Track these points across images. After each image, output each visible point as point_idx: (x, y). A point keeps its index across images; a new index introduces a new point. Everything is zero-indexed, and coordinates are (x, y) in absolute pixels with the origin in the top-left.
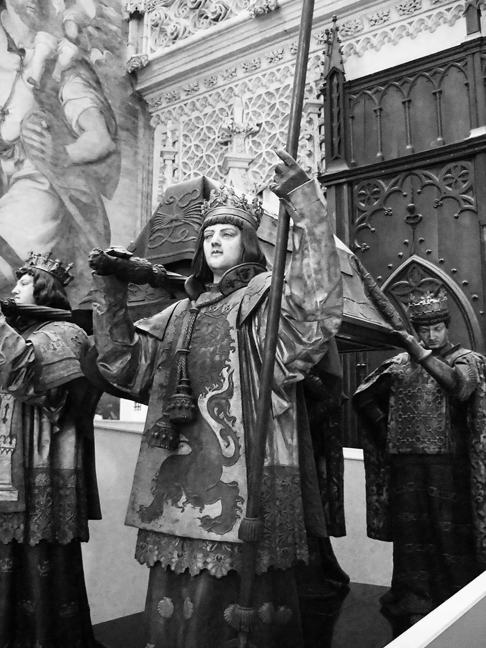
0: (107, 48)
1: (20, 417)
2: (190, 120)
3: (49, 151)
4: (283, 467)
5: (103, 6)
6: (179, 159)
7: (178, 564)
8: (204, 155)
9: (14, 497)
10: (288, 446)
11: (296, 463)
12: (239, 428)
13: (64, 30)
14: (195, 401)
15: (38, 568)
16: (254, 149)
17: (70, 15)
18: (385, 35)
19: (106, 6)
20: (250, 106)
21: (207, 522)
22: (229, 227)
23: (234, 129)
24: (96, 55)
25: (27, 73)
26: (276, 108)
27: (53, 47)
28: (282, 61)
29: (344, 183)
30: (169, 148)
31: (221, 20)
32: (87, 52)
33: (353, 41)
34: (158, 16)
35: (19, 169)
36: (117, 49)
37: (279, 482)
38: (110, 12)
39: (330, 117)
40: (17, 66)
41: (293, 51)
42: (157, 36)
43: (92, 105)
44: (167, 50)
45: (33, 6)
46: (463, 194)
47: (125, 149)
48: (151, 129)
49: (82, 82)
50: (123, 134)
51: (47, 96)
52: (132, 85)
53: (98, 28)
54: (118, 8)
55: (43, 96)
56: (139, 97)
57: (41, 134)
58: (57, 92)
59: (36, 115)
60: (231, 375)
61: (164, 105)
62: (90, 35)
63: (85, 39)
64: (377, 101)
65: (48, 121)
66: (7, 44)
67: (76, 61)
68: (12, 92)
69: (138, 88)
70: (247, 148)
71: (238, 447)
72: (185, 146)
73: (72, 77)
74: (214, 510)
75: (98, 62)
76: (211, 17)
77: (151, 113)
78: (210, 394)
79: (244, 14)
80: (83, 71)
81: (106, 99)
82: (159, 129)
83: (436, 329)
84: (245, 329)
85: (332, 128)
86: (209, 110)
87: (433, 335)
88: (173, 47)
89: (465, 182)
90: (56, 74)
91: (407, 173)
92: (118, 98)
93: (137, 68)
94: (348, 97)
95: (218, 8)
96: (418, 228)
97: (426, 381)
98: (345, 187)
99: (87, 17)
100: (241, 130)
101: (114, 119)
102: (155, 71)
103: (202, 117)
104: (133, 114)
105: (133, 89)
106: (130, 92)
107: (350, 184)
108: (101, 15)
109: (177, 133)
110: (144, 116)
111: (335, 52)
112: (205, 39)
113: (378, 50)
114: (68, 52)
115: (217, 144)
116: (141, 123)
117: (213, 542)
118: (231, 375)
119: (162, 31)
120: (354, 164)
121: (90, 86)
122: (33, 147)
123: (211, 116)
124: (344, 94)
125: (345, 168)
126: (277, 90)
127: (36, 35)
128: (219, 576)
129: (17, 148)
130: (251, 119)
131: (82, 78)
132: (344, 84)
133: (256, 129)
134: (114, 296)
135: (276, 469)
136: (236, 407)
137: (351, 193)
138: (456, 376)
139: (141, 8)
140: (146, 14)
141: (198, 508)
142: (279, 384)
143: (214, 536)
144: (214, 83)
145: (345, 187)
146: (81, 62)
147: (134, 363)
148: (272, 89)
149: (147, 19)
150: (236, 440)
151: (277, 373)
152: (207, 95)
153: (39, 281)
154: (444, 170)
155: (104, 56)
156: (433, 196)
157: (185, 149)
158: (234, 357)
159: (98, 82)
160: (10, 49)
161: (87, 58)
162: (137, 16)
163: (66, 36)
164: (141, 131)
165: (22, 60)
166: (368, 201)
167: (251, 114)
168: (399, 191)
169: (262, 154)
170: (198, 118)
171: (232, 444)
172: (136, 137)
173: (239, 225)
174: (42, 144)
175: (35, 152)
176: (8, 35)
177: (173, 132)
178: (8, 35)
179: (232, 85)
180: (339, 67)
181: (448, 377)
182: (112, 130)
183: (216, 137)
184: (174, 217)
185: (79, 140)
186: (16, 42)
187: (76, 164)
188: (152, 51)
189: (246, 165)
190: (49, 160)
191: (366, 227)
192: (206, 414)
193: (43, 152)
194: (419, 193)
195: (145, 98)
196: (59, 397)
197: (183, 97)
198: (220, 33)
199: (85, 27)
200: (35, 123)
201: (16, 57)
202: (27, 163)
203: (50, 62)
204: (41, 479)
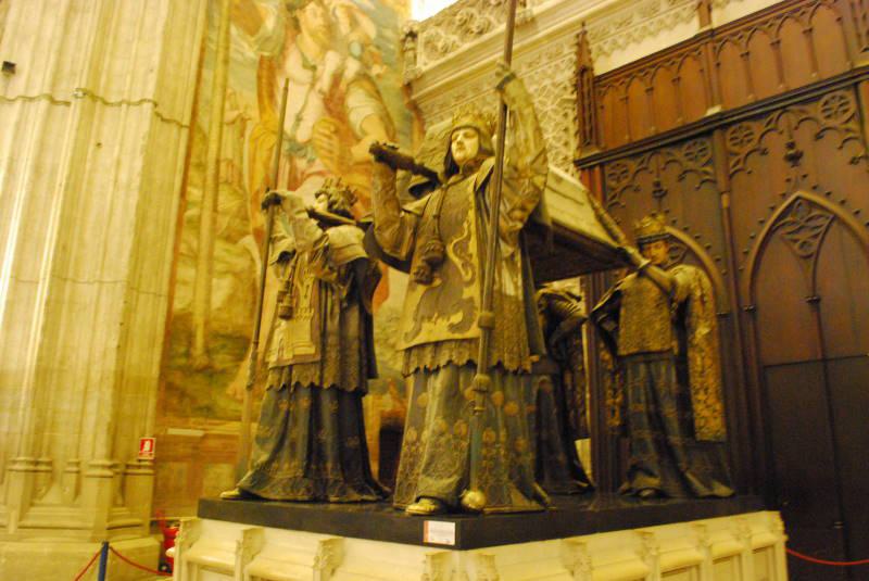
0: (386, 64)
1: (316, 293)
3: (337, 152)
4: (510, 297)
7: (432, 364)
9: (312, 350)
10: (515, 284)
11: (521, 298)
12: (475, 261)
14: (445, 247)
15: (328, 406)
17: (354, 37)
18: (629, 35)
21: (453, 328)
22: (469, 131)
24: (376, 70)
25: (318, 87)
29: (595, 166)
32: (367, 66)
33: (601, 43)
35: (311, 166)
37: (506, 307)
38: (389, 33)
39: (583, 109)
40: (310, 80)
46: (704, 165)
51: (334, 104)
53: (378, 47)
54: (395, 28)
55: (331, 105)
56: (414, 106)
57: (329, 137)
58: (343, 103)
59: (325, 120)
60: (469, 226)
62: (372, 54)
63: (367, 57)
65: (335, 125)
69: (413, 97)
71: (474, 274)
74: (457, 318)
75: (378, 76)
76: (475, 30)
78: (455, 241)
80: (367, 85)
84: (480, 195)
85: (584, 119)
87: (654, 252)
88: (443, 60)
89: (704, 156)
90: (343, 86)
91: (650, 153)
92: (396, 105)
94: (597, 90)
96: (664, 199)
97: (649, 291)
98: (597, 169)
99: (368, 38)
104: (409, 119)
106: (406, 101)
107: (602, 165)
108: (380, 35)
111: (585, 53)
112: (471, 51)
113: (624, 49)
114: (353, 67)
117: (456, 340)
118: (469, 226)
120: (605, 148)
121: (372, 96)
122: (322, 148)
124: (594, 88)
125: (597, 151)
126: (536, 90)
128: (460, 364)
129: (309, 149)
134: (387, 178)
135: (503, 296)
136: (473, 247)
137: (603, 174)
138: (674, 284)
139: (416, 29)
141: (445, 321)
142: (504, 231)
143: (458, 336)
145: (597, 169)
146: (363, 76)
147: (402, 229)
149: (421, 38)
150: (473, 269)
151: (502, 223)
153: (332, 198)
154: (686, 146)
156: (675, 170)
158: (472, 214)
159: (378, 92)
161: (368, 72)
162: (413, 35)
163: (351, 55)
164: (416, 136)
166: (618, 180)
168: (646, 169)
171: (470, 273)
172: (412, 141)
173: (477, 130)
174: (331, 145)
175: (322, 152)
176: (302, 55)
178: (302, 55)
180: (588, 65)
181: (667, 284)
182: (391, 134)
184: (431, 147)
185: (362, 142)
186: (310, 60)
187: (358, 163)
188: (425, 64)
190: (336, 158)
191: (617, 203)
192: (451, 255)
193: (331, 152)
194: (664, 169)
196: (347, 276)
199: (368, 45)
200: (325, 128)
201: (309, 73)
202: (318, 161)
203: (337, 79)
204: (332, 340)
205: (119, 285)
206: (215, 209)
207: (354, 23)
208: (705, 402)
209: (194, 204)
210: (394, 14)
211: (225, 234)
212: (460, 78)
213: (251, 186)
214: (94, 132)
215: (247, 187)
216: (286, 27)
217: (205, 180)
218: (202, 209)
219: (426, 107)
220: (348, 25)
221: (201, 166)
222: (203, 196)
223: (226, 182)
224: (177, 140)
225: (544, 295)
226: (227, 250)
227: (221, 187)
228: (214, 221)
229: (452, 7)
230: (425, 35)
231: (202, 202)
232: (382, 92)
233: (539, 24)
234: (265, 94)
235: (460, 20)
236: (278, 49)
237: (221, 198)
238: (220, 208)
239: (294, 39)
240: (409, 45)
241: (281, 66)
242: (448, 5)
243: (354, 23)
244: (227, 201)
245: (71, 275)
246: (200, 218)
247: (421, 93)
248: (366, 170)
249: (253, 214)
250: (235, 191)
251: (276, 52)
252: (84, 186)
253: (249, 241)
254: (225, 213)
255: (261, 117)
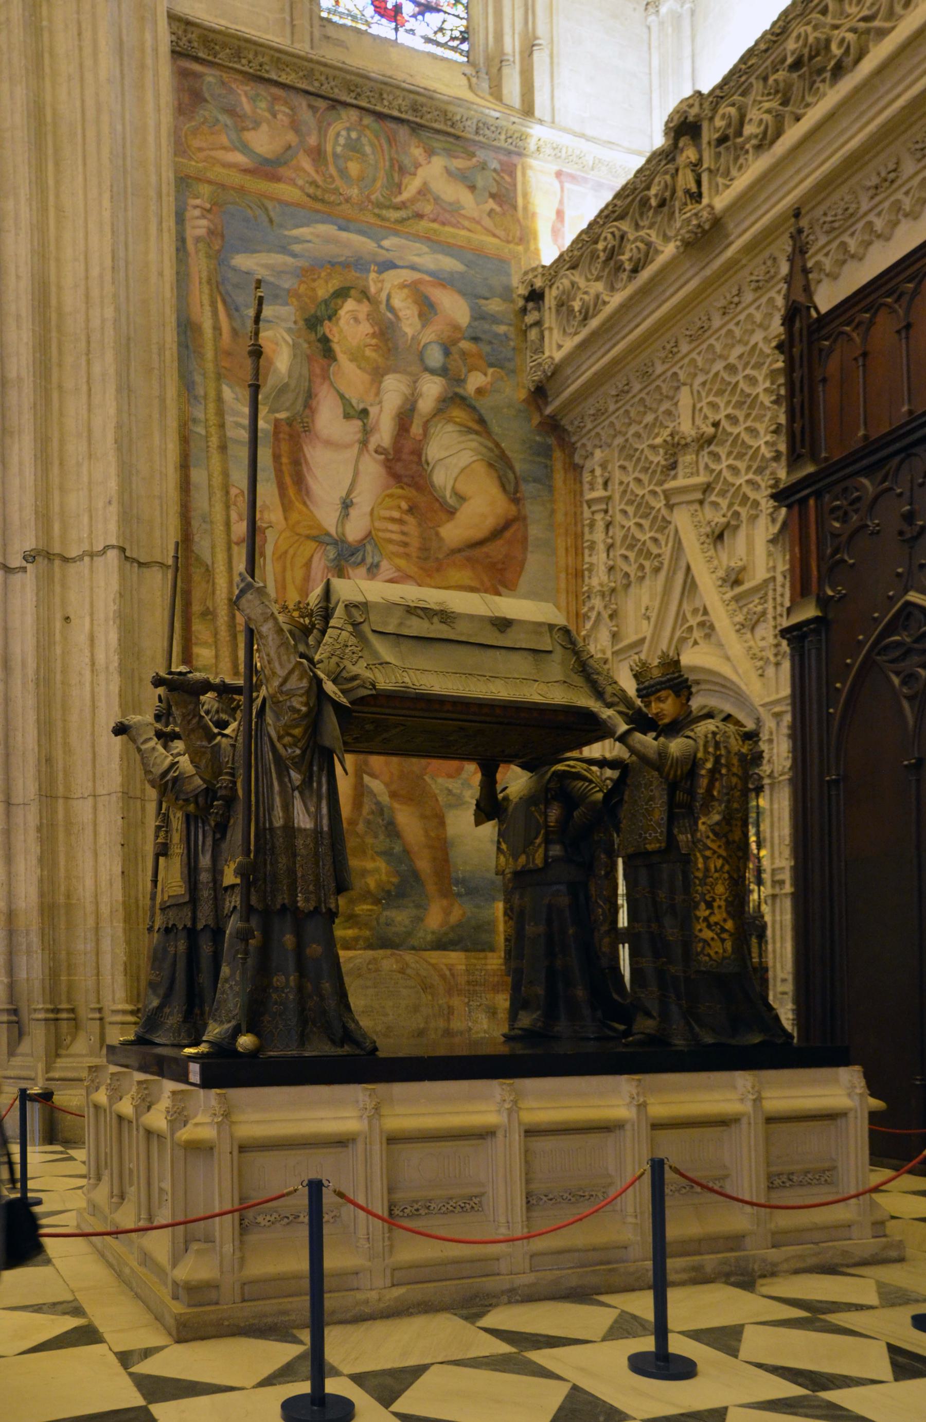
0: (491, 365)
2: (627, 440)
5: (482, 302)
6: (614, 507)
8: (646, 491)
13: (422, 360)
16: (713, 466)
19: (487, 299)
20: (704, 394)
23: (676, 439)
26: (739, 390)
27: (407, 391)
28: (740, 308)
30: (599, 493)
31: (643, 268)
34: (561, 288)
36: (509, 360)
38: (495, 306)
40: (359, 436)
42: (565, 322)
43: (474, 458)
44: (578, 339)
45: (374, 341)
47: (534, 511)
48: (576, 469)
49: (458, 428)
50: (528, 489)
52: (540, 410)
53: (475, 339)
54: (506, 294)
55: (399, 468)
56: (552, 425)
61: (589, 426)
62: (464, 354)
64: (858, 340)
66: (341, 410)
67: (444, 401)
68: (356, 474)
69: (548, 411)
70: (702, 466)
72: (621, 483)
73: (440, 426)
75: (480, 391)
77: (574, 444)
79: (669, 250)
80: (458, 414)
81: (497, 445)
82: (588, 465)
83: (659, 700)
86: (649, 418)
90: (416, 429)
92: (515, 434)
93: (541, 382)
95: (635, 250)
99: (456, 327)
100: (689, 440)
101: (512, 468)
102: (568, 378)
103: (641, 431)
104: (545, 452)
105: (541, 414)
108: (479, 316)
109: (609, 468)
110: (563, 450)
112: (624, 307)
114: (432, 389)
115: (662, 472)
116: (558, 465)
119: (571, 311)
123: (654, 425)
127: (380, 382)
130: (706, 417)
131: (456, 423)
132: (809, 327)
133: (711, 430)
140: (547, 290)
144: (650, 370)
146: (454, 399)
148: (732, 360)
149: (550, 299)
152: (643, 395)
155: (489, 379)
157: (622, 488)
159: (482, 421)
160: (347, 416)
162: (535, 296)
165: (365, 425)
167: (705, 410)
169: (720, 472)
170: (638, 435)
176: (342, 397)
177: (603, 466)
179: (676, 369)
182: (511, 488)
183: (658, 458)
189: (699, 496)
190: (414, 555)
195: (563, 423)
197: (612, 408)
198: (645, 291)
199: (455, 342)
205: (114, 798)
207: (427, 308)
208: (706, 919)
210: (502, 265)
212: (616, 362)
216: (309, 359)
219: (572, 423)
220: (416, 320)
221: (208, 614)
224: (156, 587)
225: (555, 773)
229: (591, 225)
230: (554, 292)
232: (488, 417)
233: (731, 226)
234: (288, 480)
235: (604, 250)
236: (300, 401)
239: (326, 376)
240: (530, 318)
241: (308, 429)
242: (584, 226)
243: (427, 308)
245: (61, 790)
247: (557, 403)
248: (468, 559)
251: (299, 406)
255: (286, 519)
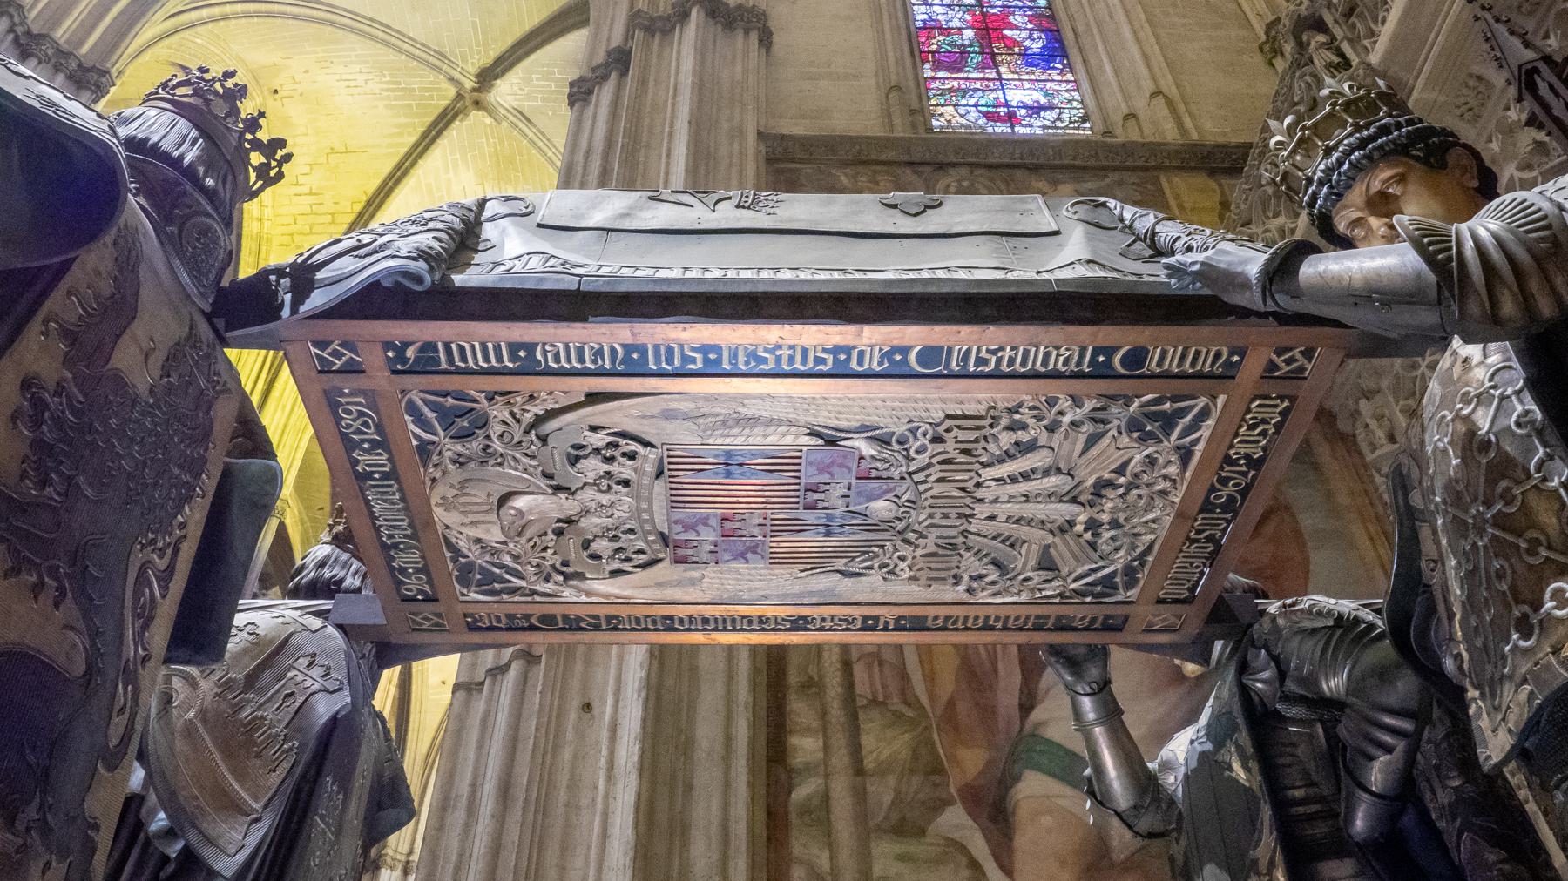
41: (1467, 116)
206: (859, 770)
209: (809, 769)
211: (895, 816)
213: (932, 697)
214: (575, 684)
215: (924, 700)
217: (824, 714)
218: (827, 776)
222: (826, 748)
223: (874, 702)
226: (902, 858)
227: (862, 716)
228: (860, 795)
231: (826, 766)
237: (868, 741)
238: (869, 763)
244: (883, 743)
246: (826, 798)
249: (952, 758)
250: (898, 716)
252: (562, 795)
253: (955, 820)
254: (884, 770)
